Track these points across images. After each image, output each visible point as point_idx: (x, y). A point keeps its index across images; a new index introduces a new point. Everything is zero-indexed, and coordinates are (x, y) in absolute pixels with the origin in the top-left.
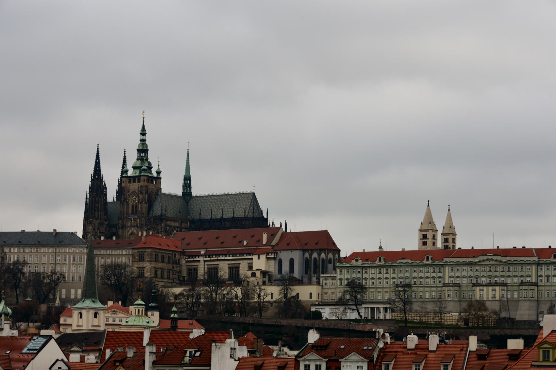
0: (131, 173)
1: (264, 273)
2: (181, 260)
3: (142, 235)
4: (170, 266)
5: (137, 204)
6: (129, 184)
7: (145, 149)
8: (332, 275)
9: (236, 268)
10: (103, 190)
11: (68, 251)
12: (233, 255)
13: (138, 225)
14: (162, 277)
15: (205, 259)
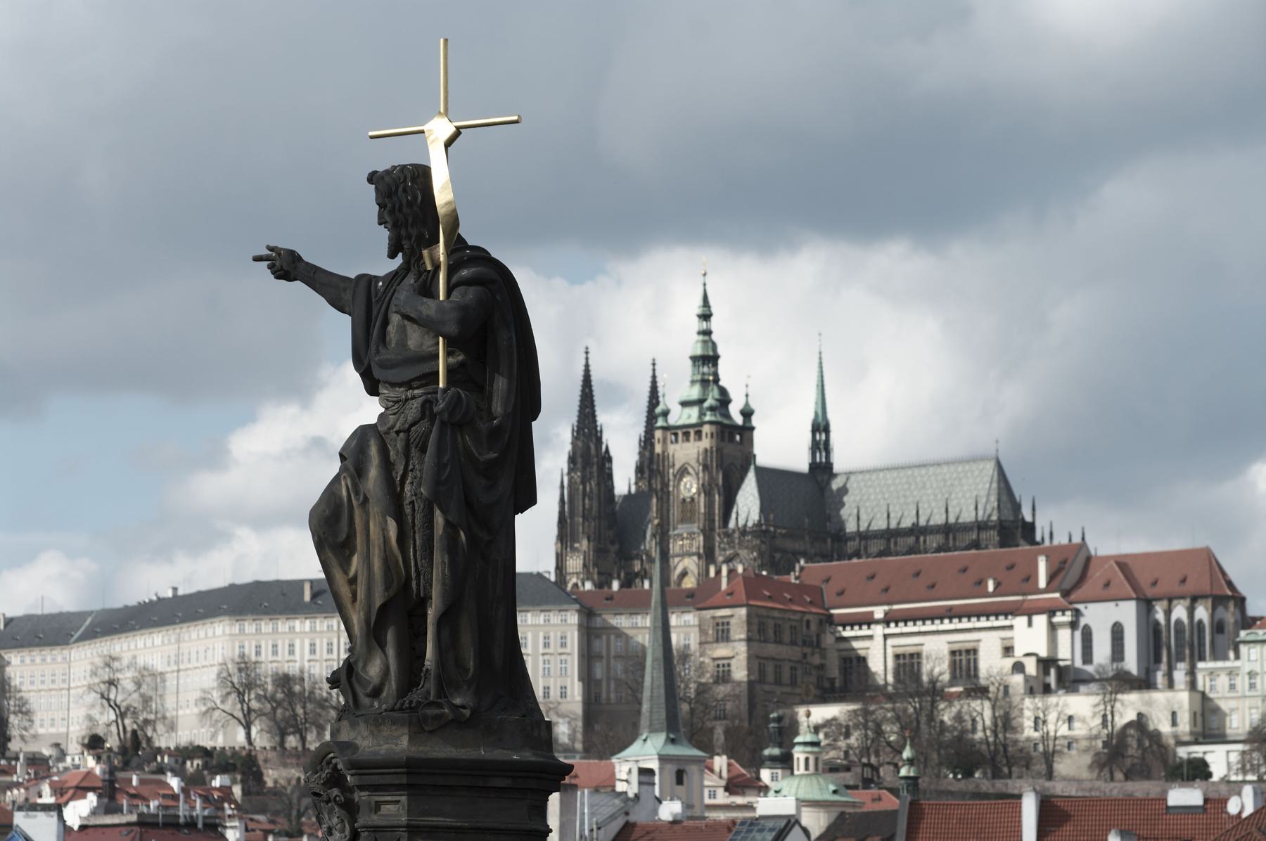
0: (680, 416)
1: (1046, 664)
2: (823, 636)
3: (718, 572)
4: (794, 653)
5: (696, 496)
6: (672, 448)
7: (711, 353)
8: (1228, 664)
9: (968, 651)
10: (604, 465)
11: (532, 621)
12: (960, 617)
13: (701, 551)
14: (778, 682)
15: (888, 631)
